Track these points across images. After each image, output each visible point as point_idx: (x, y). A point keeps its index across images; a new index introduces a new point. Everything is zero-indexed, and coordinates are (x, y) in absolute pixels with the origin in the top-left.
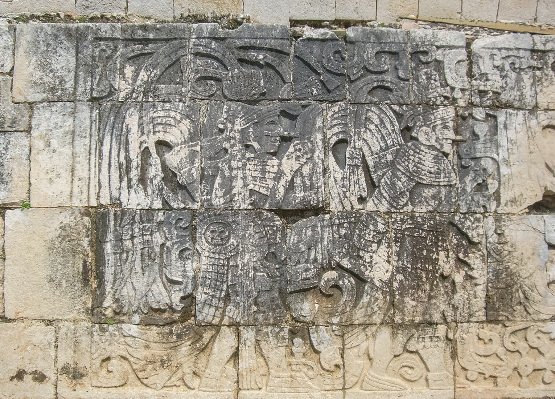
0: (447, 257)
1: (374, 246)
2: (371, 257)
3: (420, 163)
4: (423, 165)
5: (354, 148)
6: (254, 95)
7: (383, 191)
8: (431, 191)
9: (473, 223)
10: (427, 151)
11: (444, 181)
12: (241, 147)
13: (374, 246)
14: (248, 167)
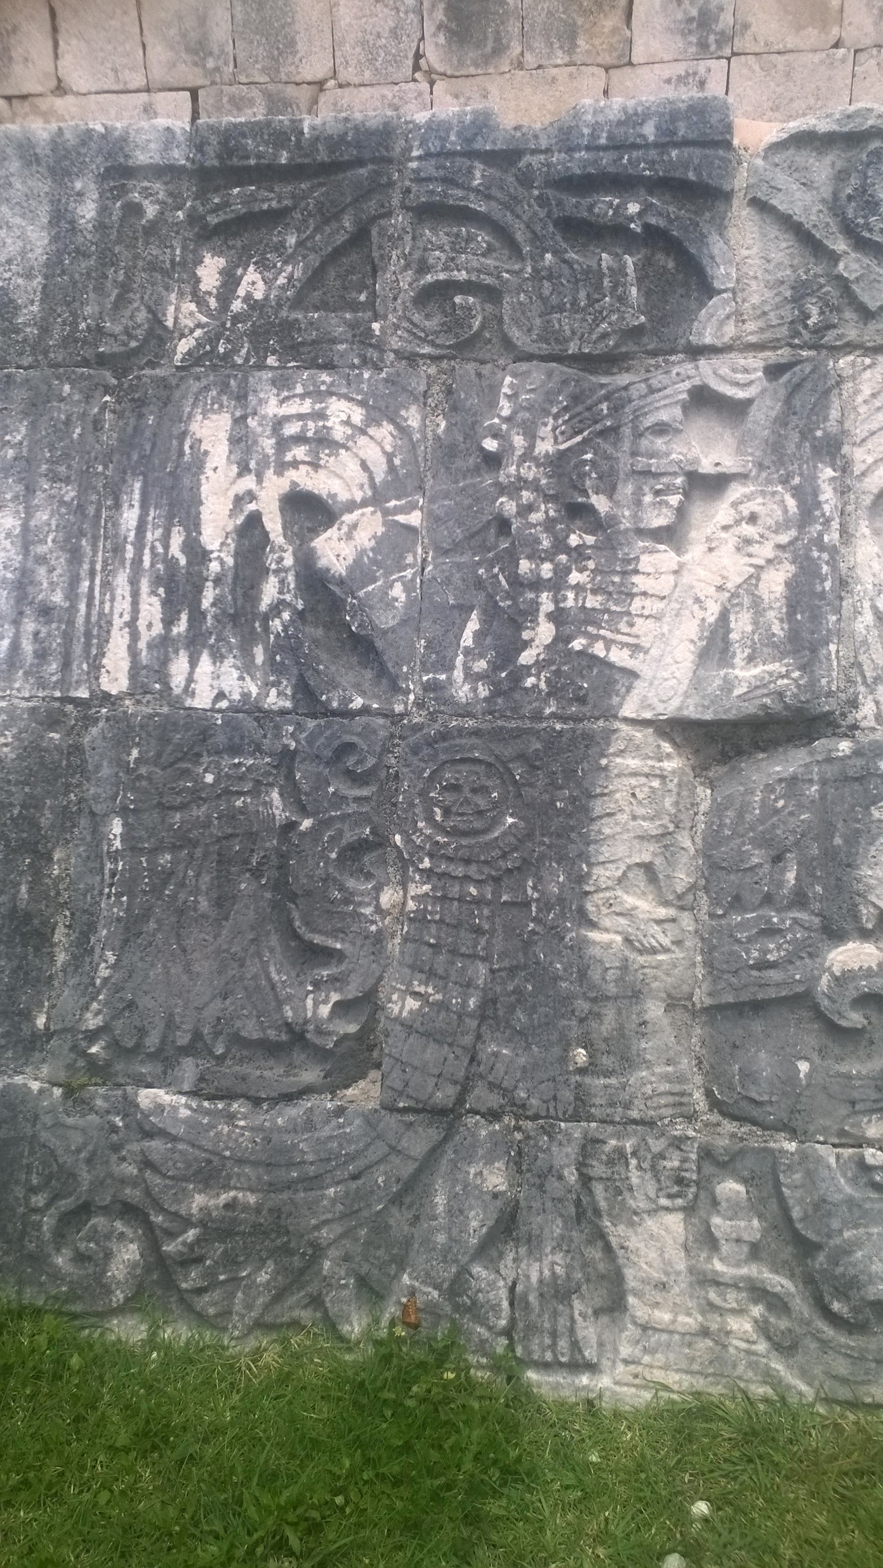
6: (604, 336)
12: (552, 513)
14: (575, 577)
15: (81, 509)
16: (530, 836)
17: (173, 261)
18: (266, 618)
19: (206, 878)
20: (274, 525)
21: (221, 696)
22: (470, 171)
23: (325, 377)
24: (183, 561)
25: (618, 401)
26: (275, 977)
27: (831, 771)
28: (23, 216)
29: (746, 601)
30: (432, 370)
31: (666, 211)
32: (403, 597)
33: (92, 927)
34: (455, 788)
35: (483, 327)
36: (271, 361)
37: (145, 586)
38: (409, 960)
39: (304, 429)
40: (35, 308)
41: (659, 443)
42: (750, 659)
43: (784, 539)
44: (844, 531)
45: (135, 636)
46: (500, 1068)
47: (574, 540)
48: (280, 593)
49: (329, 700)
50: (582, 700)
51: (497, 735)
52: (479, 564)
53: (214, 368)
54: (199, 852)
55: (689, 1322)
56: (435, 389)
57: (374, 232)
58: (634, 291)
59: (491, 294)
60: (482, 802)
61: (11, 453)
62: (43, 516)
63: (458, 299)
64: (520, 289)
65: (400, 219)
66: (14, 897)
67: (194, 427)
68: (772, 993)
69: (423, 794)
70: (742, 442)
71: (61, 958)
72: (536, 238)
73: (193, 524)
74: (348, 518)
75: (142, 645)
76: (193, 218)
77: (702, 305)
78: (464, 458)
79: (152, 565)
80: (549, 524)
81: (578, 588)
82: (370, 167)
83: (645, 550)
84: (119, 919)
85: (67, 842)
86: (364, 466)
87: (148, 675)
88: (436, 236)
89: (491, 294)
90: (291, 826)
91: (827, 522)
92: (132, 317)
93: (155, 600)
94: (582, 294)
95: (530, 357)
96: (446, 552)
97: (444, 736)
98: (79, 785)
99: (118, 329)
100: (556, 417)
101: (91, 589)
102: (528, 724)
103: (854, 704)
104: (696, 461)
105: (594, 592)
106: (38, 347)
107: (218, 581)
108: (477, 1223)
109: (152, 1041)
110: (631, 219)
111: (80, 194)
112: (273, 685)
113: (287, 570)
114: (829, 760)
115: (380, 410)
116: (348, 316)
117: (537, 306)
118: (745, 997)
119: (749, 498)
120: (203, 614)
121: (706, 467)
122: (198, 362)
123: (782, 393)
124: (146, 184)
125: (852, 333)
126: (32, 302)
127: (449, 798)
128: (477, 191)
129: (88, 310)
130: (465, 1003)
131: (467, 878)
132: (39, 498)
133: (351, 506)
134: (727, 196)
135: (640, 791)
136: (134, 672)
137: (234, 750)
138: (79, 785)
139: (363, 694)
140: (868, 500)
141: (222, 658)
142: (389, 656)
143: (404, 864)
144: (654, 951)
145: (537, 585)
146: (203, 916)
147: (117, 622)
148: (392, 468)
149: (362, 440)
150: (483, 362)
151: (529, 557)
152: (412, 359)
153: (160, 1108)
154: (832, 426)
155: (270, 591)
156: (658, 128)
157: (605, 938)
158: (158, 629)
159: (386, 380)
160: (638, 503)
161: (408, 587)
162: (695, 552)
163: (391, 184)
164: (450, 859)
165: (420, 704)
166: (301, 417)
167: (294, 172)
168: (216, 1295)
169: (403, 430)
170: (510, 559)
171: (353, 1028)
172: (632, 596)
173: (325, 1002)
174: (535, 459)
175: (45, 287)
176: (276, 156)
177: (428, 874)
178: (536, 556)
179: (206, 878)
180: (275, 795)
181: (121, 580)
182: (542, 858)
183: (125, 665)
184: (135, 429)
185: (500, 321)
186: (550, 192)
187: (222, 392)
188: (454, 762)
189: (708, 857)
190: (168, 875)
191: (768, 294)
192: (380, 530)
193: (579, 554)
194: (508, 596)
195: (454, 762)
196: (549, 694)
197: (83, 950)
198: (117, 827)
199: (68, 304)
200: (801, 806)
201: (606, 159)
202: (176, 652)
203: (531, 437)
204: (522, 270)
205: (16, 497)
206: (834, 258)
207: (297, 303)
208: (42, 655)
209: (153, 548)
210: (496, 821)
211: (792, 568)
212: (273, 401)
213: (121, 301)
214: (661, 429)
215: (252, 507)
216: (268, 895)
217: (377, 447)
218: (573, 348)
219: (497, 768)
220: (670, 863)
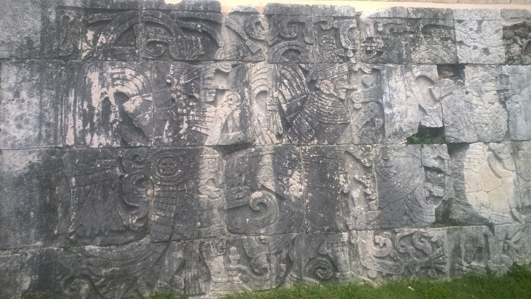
0: (346, 178)
1: (290, 171)
2: (288, 180)
3: (322, 108)
4: (324, 109)
5: (273, 97)
6: (194, 56)
7: (295, 130)
8: (331, 128)
9: (365, 152)
10: (327, 98)
11: (340, 121)
14: (192, 113)
15: (57, 97)
16: (185, 174)
17: (79, 32)
18: (112, 124)
19: (100, 191)
21: (100, 144)
22: (158, 14)
23: (124, 63)
24: (87, 110)
25: (199, 71)
26: (120, 214)
27: (251, 155)
28: (33, 17)
29: (231, 118)
30: (152, 62)
31: (207, 27)
32: (149, 118)
33: (68, 206)
34: (165, 164)
35: (164, 52)
36: (109, 59)
38: (156, 207)
39: (119, 76)
40: (39, 43)
41: (209, 82)
42: (233, 131)
43: (238, 104)
44: (250, 102)
45: (75, 130)
46: (180, 229)
47: (191, 104)
48: (115, 117)
49: (131, 144)
50: (195, 142)
51: (175, 151)
52: (168, 109)
53: (93, 60)
54: (97, 185)
55: (225, 280)
56: (153, 67)
57: (135, 28)
58: (201, 46)
59: (166, 44)
60: (172, 167)
61: (35, 82)
62: (46, 99)
63: (158, 45)
64: (173, 44)
65: (141, 25)
66: (45, 201)
67: (88, 75)
68: (240, 205)
69: (157, 166)
70: (228, 82)
71: (60, 215)
72: (176, 32)
73: (90, 100)
74: (133, 98)
75: (77, 132)
76: (84, 21)
77: (217, 50)
78: (161, 84)
79: (79, 111)
80: (185, 100)
81: (193, 115)
82: (132, 11)
83: (208, 106)
84: (76, 204)
85: (59, 185)
86: (136, 85)
87: (80, 139)
88: (151, 30)
89: (166, 44)
90: (122, 176)
91: (247, 100)
92: (68, 46)
93: (80, 120)
94: (188, 46)
95: (177, 60)
96: (159, 107)
97: (162, 152)
98: (62, 170)
99: (65, 49)
100: (184, 75)
101: (62, 118)
102: (183, 148)
103: (255, 140)
104: (218, 86)
105: (197, 116)
106: (41, 53)
107: (98, 115)
108: (175, 266)
109: (88, 234)
110: (199, 29)
111: (50, 13)
112: (115, 141)
113: (117, 112)
114: (250, 153)
115: (139, 71)
116: (129, 48)
117: (177, 49)
118: (235, 206)
119: (230, 95)
120: (94, 124)
121: (220, 87)
122: (88, 58)
123: (236, 71)
124: (69, 11)
125: (250, 58)
126: (38, 41)
127: (164, 166)
128: (160, 19)
129: (55, 44)
130: (170, 215)
131: (170, 186)
133: (133, 95)
134: (221, 25)
135: (210, 162)
136: (76, 139)
137: (105, 158)
138: (62, 170)
139: (139, 142)
140: (255, 96)
141: (100, 135)
142: (146, 133)
143: (153, 184)
144: (215, 198)
145: (183, 114)
146: (99, 201)
147: (70, 126)
148: (143, 86)
149: (135, 79)
150: (165, 61)
151: (180, 108)
152: (147, 59)
153: (91, 250)
154: (247, 79)
155: (112, 117)
156: (204, 7)
157: (204, 196)
158: (81, 128)
159: (140, 65)
160: (205, 96)
161: (150, 115)
162: (219, 107)
163: (138, 16)
164: (165, 181)
165: (155, 144)
166: (118, 73)
167: (111, 11)
168: (110, 293)
169: (146, 77)
170: (176, 108)
171: (142, 225)
172: (206, 117)
173: (134, 219)
174: (180, 85)
175: (41, 37)
176: (107, 7)
177: (160, 185)
178: (182, 108)
179: (100, 191)
180: (117, 169)
181: (70, 115)
182: (188, 179)
183: (73, 138)
184: (72, 76)
185: (169, 51)
186: (178, 21)
187: (96, 66)
188: (165, 158)
189: (226, 176)
190: (89, 191)
191: (231, 48)
192: (141, 101)
193: (192, 107)
194: (176, 117)
195: (165, 158)
196: (187, 140)
197: (66, 212)
198: (74, 180)
199: (49, 42)
200: (245, 163)
201: (192, 14)
202: (87, 133)
203: (179, 80)
204: (173, 39)
205: (37, 94)
206: (245, 41)
207: (115, 44)
208: (48, 136)
209: (79, 107)
210: (176, 171)
211: (240, 111)
212: (110, 69)
213: (65, 42)
214: (209, 78)
215: (106, 96)
216: (117, 194)
217: (139, 81)
218: (187, 59)
219: (176, 159)
220: (218, 178)
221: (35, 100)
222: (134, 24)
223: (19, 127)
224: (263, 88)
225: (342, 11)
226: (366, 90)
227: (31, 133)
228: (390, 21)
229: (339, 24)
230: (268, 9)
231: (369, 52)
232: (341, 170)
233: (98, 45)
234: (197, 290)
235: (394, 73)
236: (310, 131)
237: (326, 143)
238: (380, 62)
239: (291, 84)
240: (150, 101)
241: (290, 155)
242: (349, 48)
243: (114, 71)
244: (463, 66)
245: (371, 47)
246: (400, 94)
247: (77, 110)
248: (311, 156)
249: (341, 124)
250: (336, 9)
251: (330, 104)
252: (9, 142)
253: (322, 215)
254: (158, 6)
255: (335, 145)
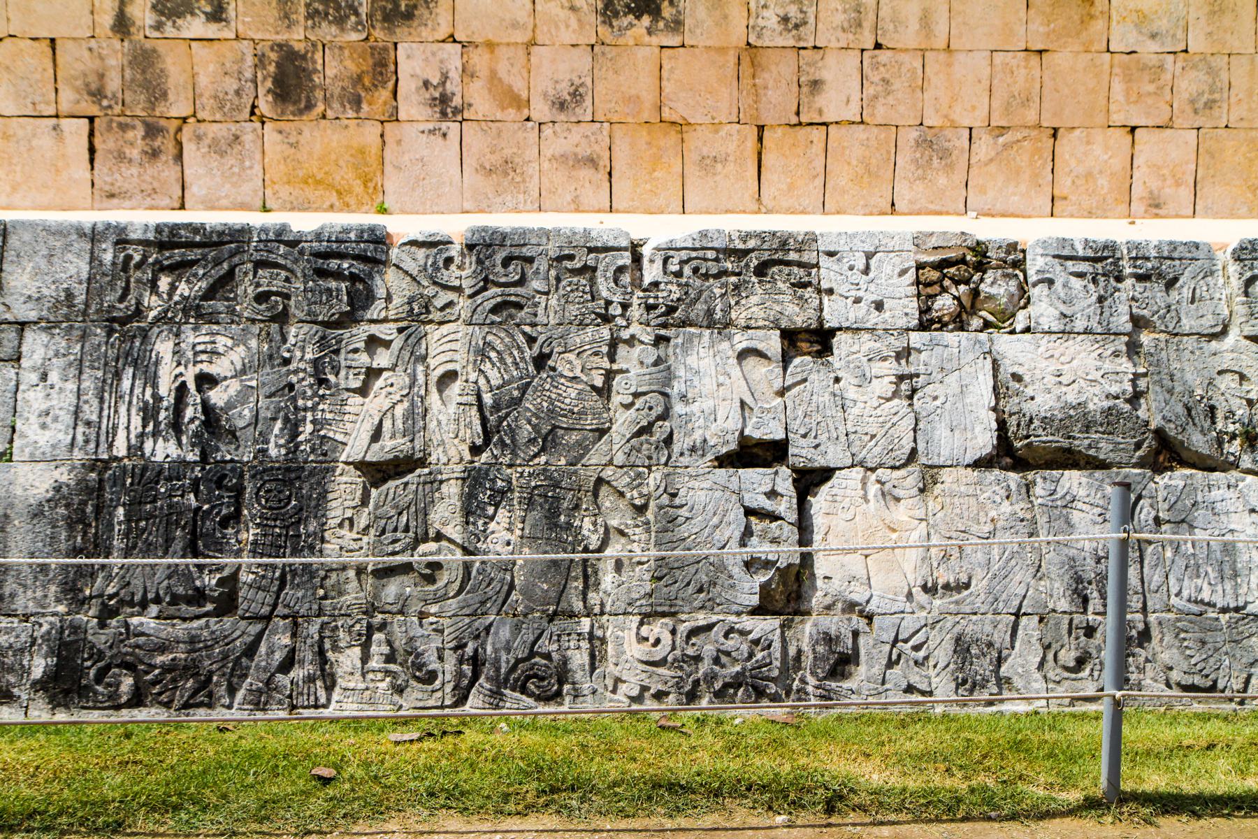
0: (595, 524)
1: (491, 510)
13: (491, 510)
14: (321, 407)
15: (104, 381)
16: (301, 509)
20: (192, 386)
21: (168, 456)
23: (215, 327)
31: (359, 268)
37: (134, 411)
50: (325, 455)
53: (166, 323)
67: (156, 347)
72: (305, 276)
73: (155, 386)
80: (311, 386)
81: (323, 410)
87: (135, 450)
89: (287, 297)
95: (303, 322)
107: (167, 409)
108: (278, 656)
117: (305, 303)
122: (159, 320)
132: (84, 377)
133: (225, 378)
145: (305, 409)
153: (142, 624)
155: (189, 413)
161: (251, 411)
168: (168, 693)
177: (258, 525)
181: (123, 410)
183: (126, 444)
190: (144, 530)
208: (87, 441)
217: (238, 356)
218: (320, 318)
221: (71, 386)
222: (236, 266)
223: (44, 426)
224: (450, 367)
225: (605, 238)
226: (645, 371)
227: (61, 436)
228: (694, 254)
229: (597, 260)
230: (470, 235)
231: (650, 308)
232: (586, 510)
233: (176, 298)
234: (312, 698)
235: (696, 343)
236: (532, 441)
237: (563, 462)
238: (672, 325)
239: (502, 360)
240: (252, 387)
241: (493, 481)
242: (615, 299)
243: (198, 340)
244: (832, 332)
245: (657, 297)
246: (706, 380)
247: (135, 401)
248: (533, 484)
249: (591, 430)
250: (594, 234)
251: (573, 396)
252: (27, 450)
253: (545, 586)
254: (280, 235)
255: (579, 466)
